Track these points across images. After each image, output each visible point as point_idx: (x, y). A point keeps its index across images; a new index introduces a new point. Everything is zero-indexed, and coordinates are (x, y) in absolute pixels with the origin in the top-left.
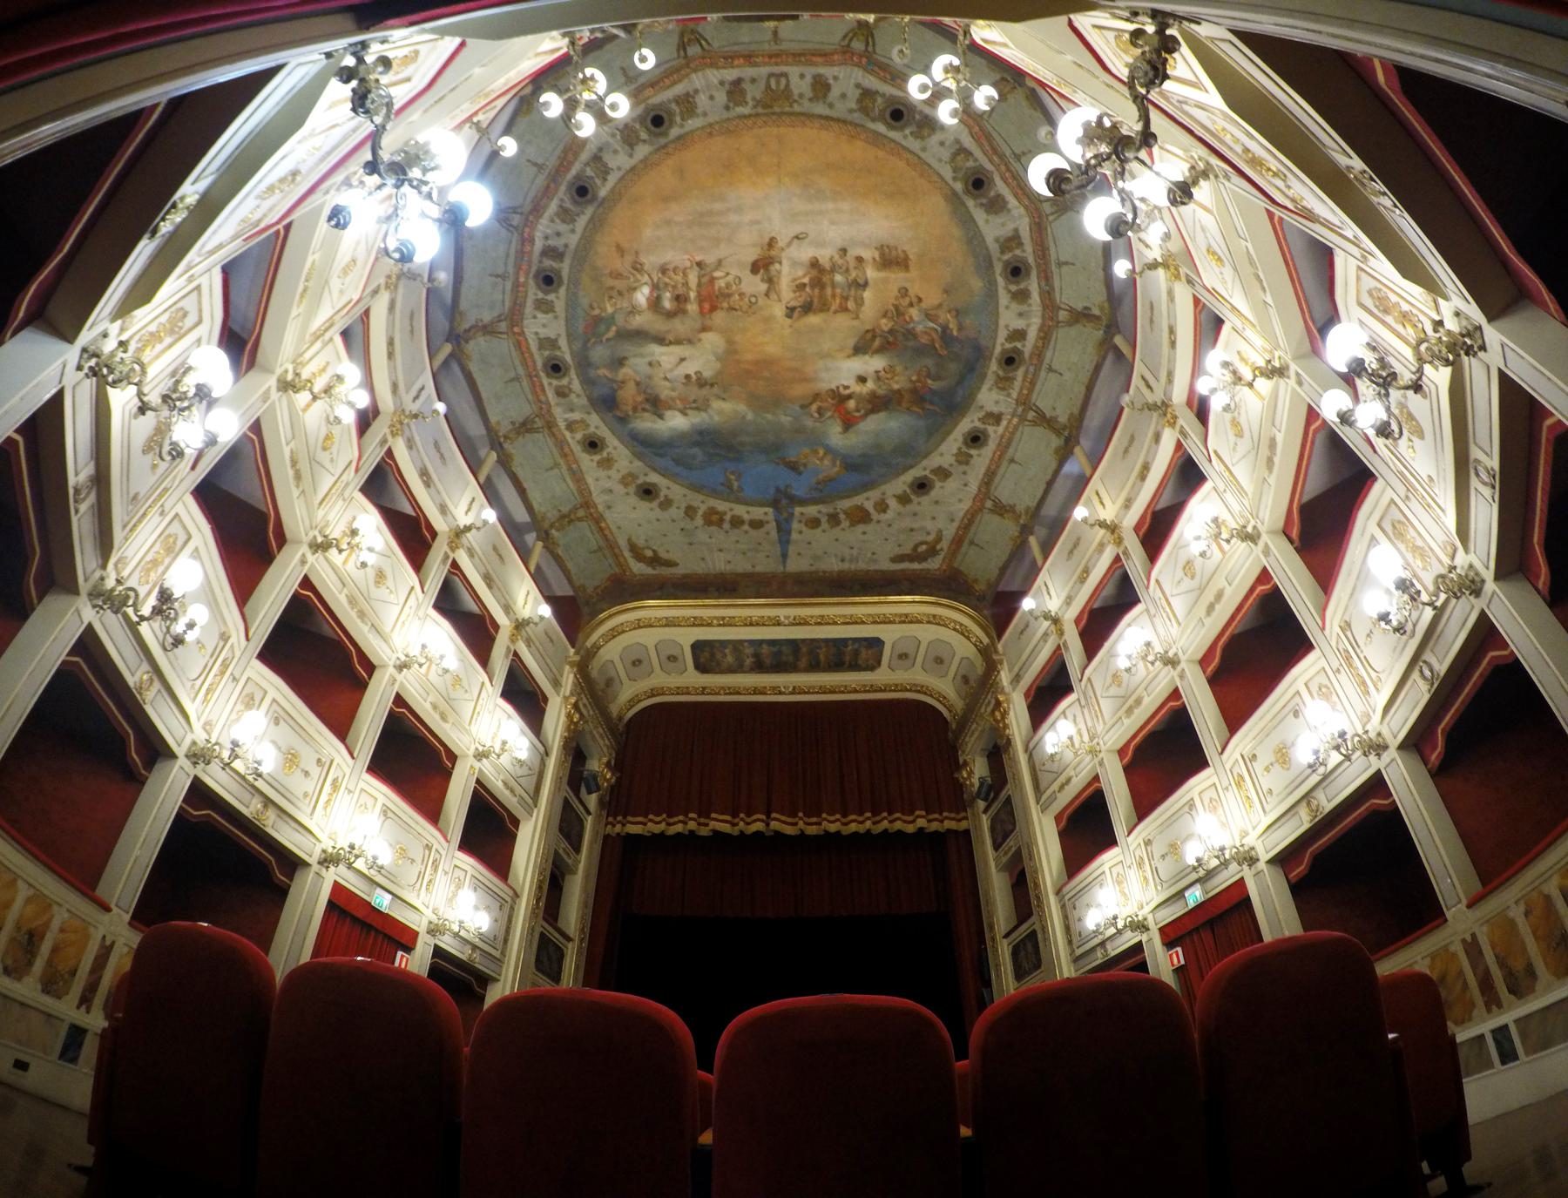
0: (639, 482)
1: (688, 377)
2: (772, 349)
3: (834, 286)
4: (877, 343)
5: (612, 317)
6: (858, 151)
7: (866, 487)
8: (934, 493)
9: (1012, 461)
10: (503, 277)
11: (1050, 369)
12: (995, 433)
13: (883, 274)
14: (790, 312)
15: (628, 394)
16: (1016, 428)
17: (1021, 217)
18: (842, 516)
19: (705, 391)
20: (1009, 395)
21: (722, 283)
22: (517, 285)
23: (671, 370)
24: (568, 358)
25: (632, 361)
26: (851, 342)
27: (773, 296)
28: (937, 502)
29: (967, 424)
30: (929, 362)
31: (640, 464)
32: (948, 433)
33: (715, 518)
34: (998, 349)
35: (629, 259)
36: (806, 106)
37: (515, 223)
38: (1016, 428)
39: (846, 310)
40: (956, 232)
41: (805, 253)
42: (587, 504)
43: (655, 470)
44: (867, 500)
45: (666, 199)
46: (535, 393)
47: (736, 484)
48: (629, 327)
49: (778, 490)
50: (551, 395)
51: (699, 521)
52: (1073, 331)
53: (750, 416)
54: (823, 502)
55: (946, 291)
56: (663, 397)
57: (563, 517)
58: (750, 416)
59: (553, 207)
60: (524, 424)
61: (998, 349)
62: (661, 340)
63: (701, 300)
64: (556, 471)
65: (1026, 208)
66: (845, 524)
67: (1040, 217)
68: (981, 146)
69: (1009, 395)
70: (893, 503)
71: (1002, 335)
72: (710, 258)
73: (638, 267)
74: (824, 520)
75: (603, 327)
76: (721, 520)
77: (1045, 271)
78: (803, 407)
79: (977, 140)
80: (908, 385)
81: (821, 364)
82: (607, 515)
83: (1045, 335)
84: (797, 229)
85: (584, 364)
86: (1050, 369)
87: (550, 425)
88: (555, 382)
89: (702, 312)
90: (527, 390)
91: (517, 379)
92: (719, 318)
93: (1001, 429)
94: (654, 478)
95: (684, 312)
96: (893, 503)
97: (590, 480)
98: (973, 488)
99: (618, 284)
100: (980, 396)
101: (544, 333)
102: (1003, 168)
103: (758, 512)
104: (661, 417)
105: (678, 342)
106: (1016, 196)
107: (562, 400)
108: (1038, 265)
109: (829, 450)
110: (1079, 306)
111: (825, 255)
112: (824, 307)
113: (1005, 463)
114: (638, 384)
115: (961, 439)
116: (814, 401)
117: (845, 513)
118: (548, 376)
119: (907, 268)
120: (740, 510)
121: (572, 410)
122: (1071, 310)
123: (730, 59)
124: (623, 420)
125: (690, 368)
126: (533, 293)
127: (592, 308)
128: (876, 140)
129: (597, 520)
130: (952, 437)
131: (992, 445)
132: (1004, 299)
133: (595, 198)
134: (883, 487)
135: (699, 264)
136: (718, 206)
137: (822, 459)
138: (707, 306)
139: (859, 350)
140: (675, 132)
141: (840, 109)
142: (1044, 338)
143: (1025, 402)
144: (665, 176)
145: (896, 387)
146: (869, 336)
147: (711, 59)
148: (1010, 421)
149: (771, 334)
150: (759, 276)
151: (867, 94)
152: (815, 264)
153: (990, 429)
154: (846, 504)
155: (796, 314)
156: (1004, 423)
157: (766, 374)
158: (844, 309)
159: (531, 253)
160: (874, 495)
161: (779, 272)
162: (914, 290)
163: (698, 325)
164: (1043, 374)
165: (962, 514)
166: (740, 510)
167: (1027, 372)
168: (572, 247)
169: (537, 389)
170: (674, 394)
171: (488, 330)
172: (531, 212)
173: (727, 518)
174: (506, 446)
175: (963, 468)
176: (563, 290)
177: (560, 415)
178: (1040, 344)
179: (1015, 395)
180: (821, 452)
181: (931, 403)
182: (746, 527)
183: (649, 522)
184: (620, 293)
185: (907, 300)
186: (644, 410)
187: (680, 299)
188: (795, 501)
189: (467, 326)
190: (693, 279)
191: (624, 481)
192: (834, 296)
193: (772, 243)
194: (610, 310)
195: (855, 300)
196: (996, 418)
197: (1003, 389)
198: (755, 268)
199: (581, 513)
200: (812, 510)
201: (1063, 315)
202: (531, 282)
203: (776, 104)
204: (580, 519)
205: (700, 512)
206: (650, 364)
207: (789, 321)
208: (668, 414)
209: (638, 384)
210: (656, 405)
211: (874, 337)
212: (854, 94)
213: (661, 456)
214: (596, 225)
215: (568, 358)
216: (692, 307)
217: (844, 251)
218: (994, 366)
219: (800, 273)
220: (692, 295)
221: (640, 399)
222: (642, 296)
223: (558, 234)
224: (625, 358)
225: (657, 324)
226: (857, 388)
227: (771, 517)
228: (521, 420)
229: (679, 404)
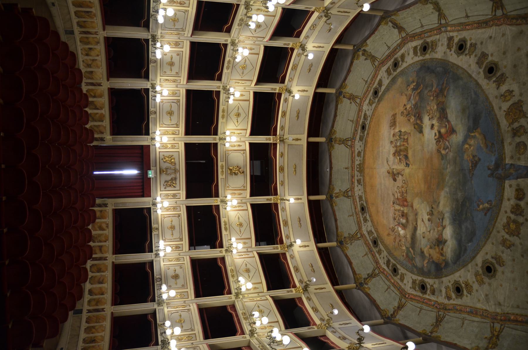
0: (481, 271)
1: (429, 220)
2: (420, 174)
3: (400, 146)
4: (418, 122)
5: (407, 248)
6: (370, 140)
7: (490, 110)
8: (495, 59)
9: (467, 16)
10: (389, 287)
11: (422, 26)
12: (457, 36)
13: (397, 124)
14: (407, 165)
15: (435, 254)
16: (452, 25)
17: (382, 72)
18: (516, 125)
19: (435, 213)
20: (439, 40)
21: (399, 195)
22: (393, 284)
23: (426, 227)
24: (420, 278)
25: (422, 247)
26: (418, 135)
27: (402, 173)
28: (504, 53)
29: (453, 58)
30: (426, 92)
31: (470, 265)
32: (458, 66)
33: (513, 226)
34: (421, 58)
35: (391, 233)
36: (362, 159)
37: (377, 272)
38: (452, 25)
39: (407, 139)
40: (386, 96)
41: (391, 158)
42: (494, 317)
43: (474, 257)
44: (501, 109)
45: (378, 212)
46: (429, 305)
47: (486, 205)
48: (410, 242)
49: (491, 175)
50: (433, 298)
51: (515, 240)
52: (405, 26)
53: (447, 189)
54: (502, 142)
55: (402, 95)
56: (437, 236)
57: (491, 338)
58: (447, 189)
59: (377, 255)
60: (437, 320)
61: (421, 58)
62: (415, 229)
63: (404, 206)
64: (466, 322)
65: (379, 71)
66: (523, 121)
67: (380, 64)
68: (367, 96)
69: (439, 40)
70: (504, 88)
71: (417, 59)
72: (392, 199)
73: (393, 230)
74: (517, 140)
75: (410, 254)
76: (515, 222)
77: (393, 52)
78: (442, 159)
79: (366, 98)
80: (435, 101)
81: (425, 150)
82: (507, 310)
83: (413, 37)
84: (386, 162)
85: (421, 272)
86: (422, 26)
87: (445, 308)
88: (428, 292)
89: (407, 206)
90: (427, 308)
91: (421, 309)
92: (409, 199)
93: (454, 34)
94: (479, 260)
95: (407, 214)
96: (504, 88)
97: (479, 306)
98: (491, 31)
99: (397, 240)
100: (440, 57)
101: (410, 285)
102: (371, 85)
103: (509, 192)
104: (446, 241)
105: (416, 221)
106: (377, 77)
107: (436, 293)
108: (393, 56)
109: (465, 142)
110: (396, 31)
111: (392, 150)
112: (406, 150)
113: (471, 19)
114: (431, 248)
115: (461, 57)
116: (440, 152)
117: (512, 123)
118: (425, 293)
119: (396, 114)
120: (507, 205)
121: (441, 291)
122: (400, 32)
123: (353, 183)
124: (447, 264)
125: (426, 217)
126: (397, 279)
127: (403, 256)
128: (368, 134)
129: (506, 319)
130: (460, 64)
131: (465, 34)
132: (405, 65)
133: (376, 238)
134: (491, 98)
135: (394, 203)
136: (380, 192)
137: (470, 145)
138: (405, 203)
139: (420, 130)
140: (365, 204)
141: (362, 148)
142: (414, 37)
143: (439, 29)
144: (373, 209)
145: (435, 107)
146: (416, 126)
147: (352, 189)
148: (450, 31)
149: (414, 174)
150: (397, 178)
151: (361, 139)
152: (394, 154)
153: (456, 40)
154: (504, 123)
155: (408, 162)
156: (451, 34)
157: (429, 178)
158: (407, 140)
159: (387, 272)
160: (495, 103)
161: (396, 170)
162: (402, 109)
163: (411, 208)
164: (426, 28)
165: (514, 28)
166: (507, 205)
167: (427, 37)
168: (387, 254)
169: (427, 303)
170: (436, 230)
171: (400, 307)
172: (377, 265)
173: (513, 216)
174: (433, 335)
175: (479, 46)
176: (399, 266)
177: (442, 299)
178: (416, 37)
179: (438, 37)
180: (466, 146)
181: (443, 84)
182: (522, 203)
183: (514, 280)
184: (400, 241)
185: (405, 111)
186: (442, 249)
187: (403, 215)
188: (499, 163)
189: (392, 313)
190: (397, 207)
191: (481, 283)
192: (403, 145)
193: (389, 173)
194: (404, 248)
195: (405, 135)
196: (450, 39)
197: (436, 45)
198: (395, 180)
199: (497, 326)
200: (508, 150)
201: (404, 35)
202: (395, 278)
203: (361, 169)
204: (501, 331)
205: (507, 236)
206: (424, 237)
207: (410, 165)
208: (444, 236)
209: (431, 248)
210: (440, 242)
211: (417, 124)
212: (361, 143)
213: (466, 250)
214: (383, 242)
215: (420, 278)
216: (406, 210)
217: (391, 142)
218: (427, 56)
219: (396, 160)
220: (402, 209)
221: (437, 250)
222: (402, 232)
223: (384, 258)
224: (421, 249)
225: (410, 227)
226: (436, 128)
227: (514, 182)
228: (435, 321)
229: (440, 228)
